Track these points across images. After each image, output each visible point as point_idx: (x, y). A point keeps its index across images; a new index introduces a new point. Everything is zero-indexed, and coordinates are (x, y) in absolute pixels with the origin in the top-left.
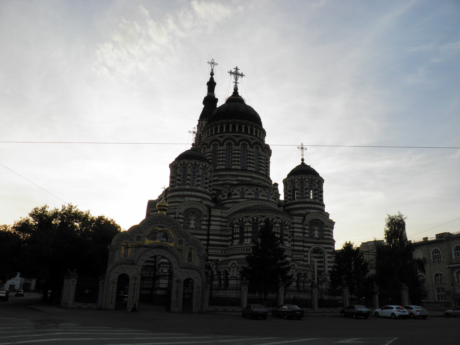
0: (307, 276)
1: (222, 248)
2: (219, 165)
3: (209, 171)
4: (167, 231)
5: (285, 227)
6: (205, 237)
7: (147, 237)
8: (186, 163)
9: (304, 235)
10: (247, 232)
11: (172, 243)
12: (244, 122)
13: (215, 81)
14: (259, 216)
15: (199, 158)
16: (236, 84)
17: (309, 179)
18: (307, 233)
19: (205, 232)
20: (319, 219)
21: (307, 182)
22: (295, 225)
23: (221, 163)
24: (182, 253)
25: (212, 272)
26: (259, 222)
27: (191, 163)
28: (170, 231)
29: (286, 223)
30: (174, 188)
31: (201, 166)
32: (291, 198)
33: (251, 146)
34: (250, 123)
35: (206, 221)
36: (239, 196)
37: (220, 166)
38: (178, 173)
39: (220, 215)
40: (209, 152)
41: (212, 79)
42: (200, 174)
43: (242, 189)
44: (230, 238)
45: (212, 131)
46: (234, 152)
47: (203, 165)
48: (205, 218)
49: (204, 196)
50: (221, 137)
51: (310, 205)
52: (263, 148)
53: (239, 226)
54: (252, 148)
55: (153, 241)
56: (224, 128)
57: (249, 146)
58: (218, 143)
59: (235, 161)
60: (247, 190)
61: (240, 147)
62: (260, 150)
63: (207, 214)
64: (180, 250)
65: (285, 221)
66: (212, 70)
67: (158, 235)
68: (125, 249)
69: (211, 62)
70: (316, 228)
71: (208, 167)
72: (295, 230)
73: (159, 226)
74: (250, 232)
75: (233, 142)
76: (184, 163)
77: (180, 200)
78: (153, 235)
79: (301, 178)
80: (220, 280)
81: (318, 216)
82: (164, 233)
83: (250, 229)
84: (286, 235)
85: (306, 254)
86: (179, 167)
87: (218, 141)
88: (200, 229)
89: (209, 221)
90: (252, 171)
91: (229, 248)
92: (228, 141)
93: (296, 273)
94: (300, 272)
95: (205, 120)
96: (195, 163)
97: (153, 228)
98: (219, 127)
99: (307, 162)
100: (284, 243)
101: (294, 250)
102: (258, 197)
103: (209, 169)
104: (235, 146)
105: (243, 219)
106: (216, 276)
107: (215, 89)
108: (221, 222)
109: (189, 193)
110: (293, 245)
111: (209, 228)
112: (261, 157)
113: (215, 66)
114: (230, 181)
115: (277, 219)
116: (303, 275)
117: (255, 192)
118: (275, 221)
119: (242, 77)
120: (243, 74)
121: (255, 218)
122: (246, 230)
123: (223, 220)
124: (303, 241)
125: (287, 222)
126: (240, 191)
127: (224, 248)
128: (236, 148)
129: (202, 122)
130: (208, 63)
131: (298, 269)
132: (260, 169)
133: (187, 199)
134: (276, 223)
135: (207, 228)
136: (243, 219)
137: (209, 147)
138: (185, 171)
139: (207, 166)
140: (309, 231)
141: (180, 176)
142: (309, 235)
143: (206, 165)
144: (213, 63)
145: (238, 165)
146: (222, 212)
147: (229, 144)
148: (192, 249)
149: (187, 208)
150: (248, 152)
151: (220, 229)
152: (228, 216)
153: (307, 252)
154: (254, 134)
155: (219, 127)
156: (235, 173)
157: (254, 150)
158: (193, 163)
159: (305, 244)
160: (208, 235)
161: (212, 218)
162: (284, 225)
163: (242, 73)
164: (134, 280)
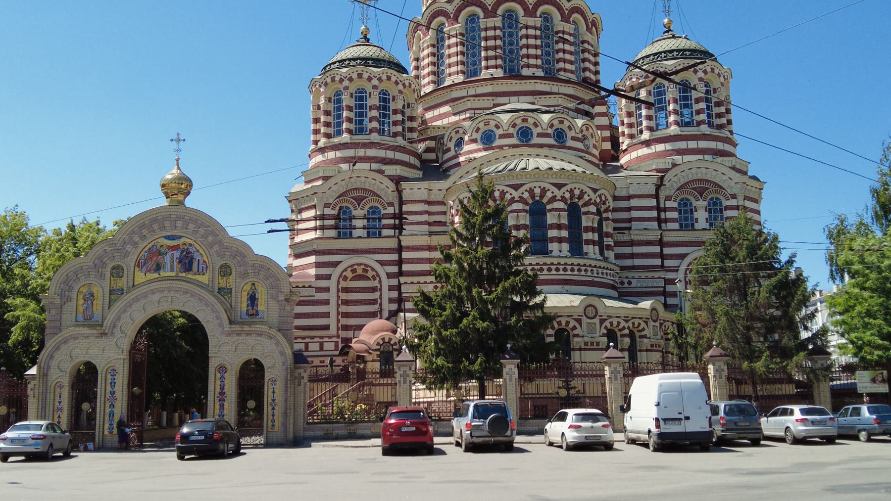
0: (643, 333)
3: (400, 92)
4: (191, 245)
5: (584, 210)
6: (395, 257)
7: (138, 266)
9: (663, 225)
11: (203, 274)
14: (507, 186)
15: (370, 62)
18: (673, 220)
19: (392, 243)
20: (708, 177)
22: (634, 203)
24: (231, 296)
26: (526, 205)
27: (349, 76)
28: (196, 245)
29: (586, 198)
31: (375, 82)
37: (453, 77)
39: (427, 199)
46: (483, 34)
48: (390, 210)
52: (567, 12)
54: (531, 16)
55: (156, 275)
57: (521, 12)
61: (497, 21)
63: (393, 197)
64: (225, 292)
65: (582, 193)
67: (168, 258)
68: (85, 300)
70: (698, 203)
71: (397, 83)
72: (635, 214)
73: (169, 236)
78: (154, 259)
81: (704, 171)
82: (182, 253)
84: (587, 229)
85: (670, 276)
88: (380, 236)
93: (603, 326)
94: (615, 324)
96: (360, 76)
97: (152, 243)
100: (585, 251)
101: (633, 268)
102: (530, 140)
103: (400, 87)
104: (485, 20)
108: (430, 213)
110: (632, 256)
114: (476, 111)
116: (626, 332)
117: (520, 129)
118: (549, 195)
124: (661, 243)
125: (589, 196)
126: (481, 132)
128: (489, 25)
131: (611, 317)
132: (559, 70)
134: (553, 199)
135: (397, 234)
139: (393, 79)
140: (680, 213)
142: (681, 225)
143: (389, 78)
145: (496, 67)
148: (256, 283)
149: (342, 190)
151: (428, 233)
153: (676, 270)
156: (488, 88)
157: (538, 21)
159: (667, 251)
160: (400, 249)
161: (405, 208)
162: (580, 203)
164: (111, 375)
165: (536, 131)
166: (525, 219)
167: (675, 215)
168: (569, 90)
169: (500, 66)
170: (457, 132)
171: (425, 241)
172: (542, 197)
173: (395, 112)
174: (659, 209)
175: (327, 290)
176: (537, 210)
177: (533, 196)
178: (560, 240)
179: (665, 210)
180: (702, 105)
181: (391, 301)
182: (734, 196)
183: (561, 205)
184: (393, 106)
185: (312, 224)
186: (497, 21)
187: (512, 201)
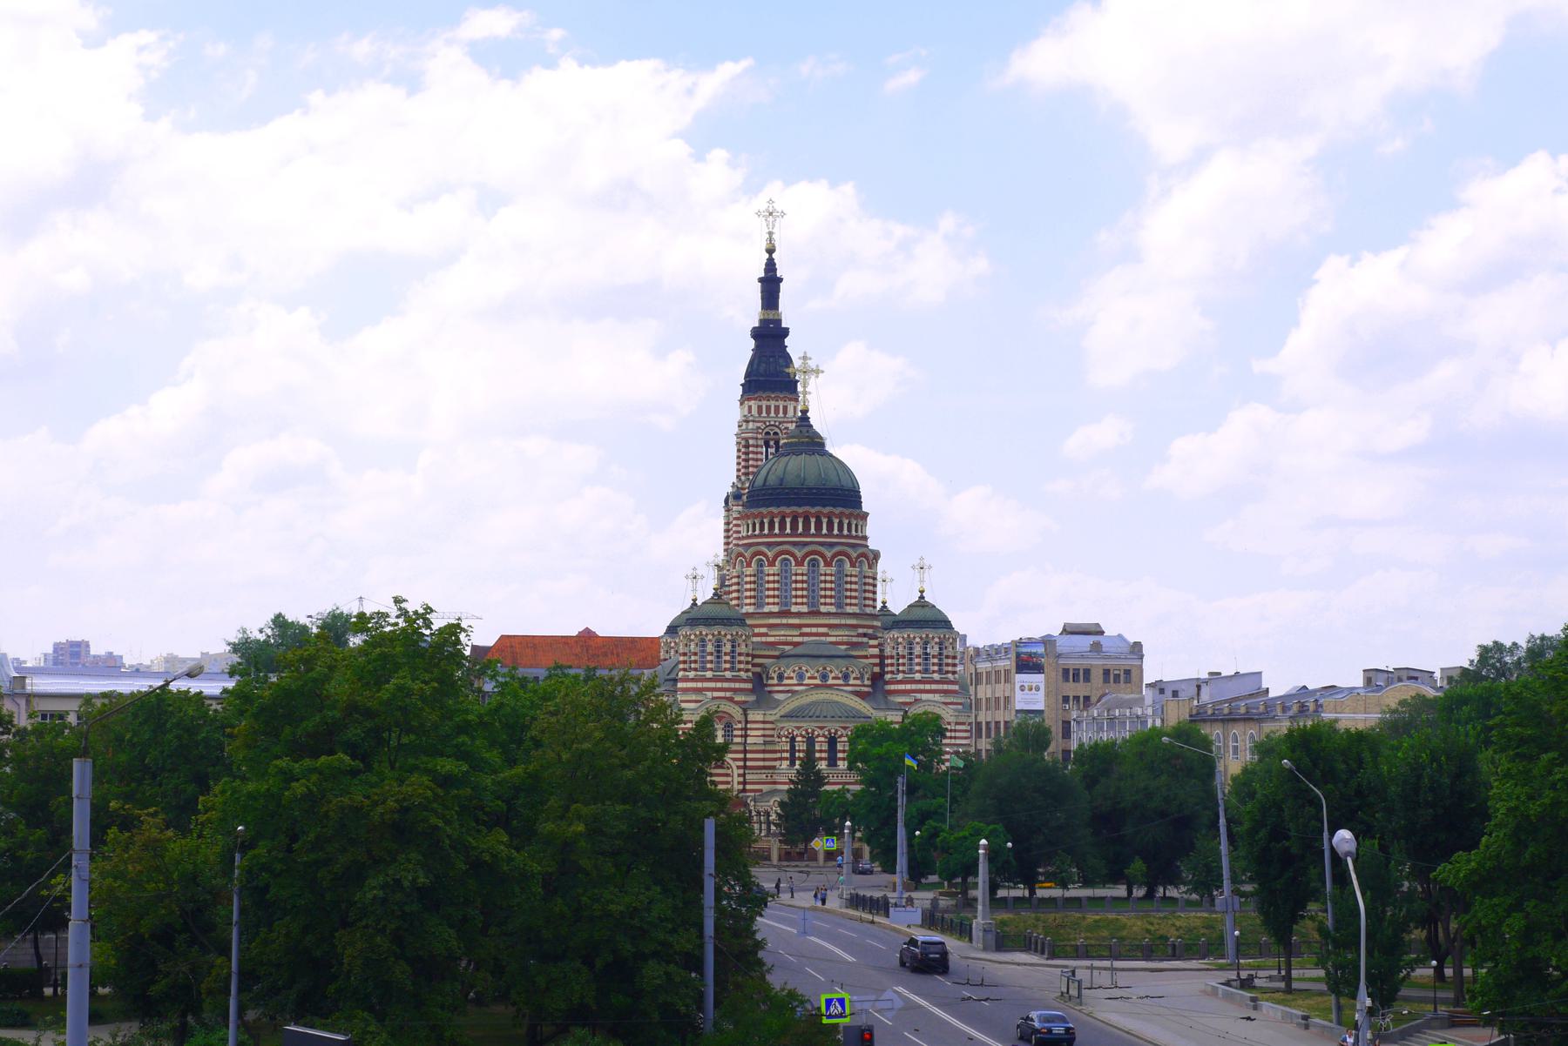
1: (766, 771)
2: (768, 604)
3: (744, 641)
6: (741, 756)
8: (704, 633)
10: (799, 751)
12: (813, 510)
16: (804, 397)
17: (921, 638)
19: (741, 748)
21: (918, 643)
23: (771, 600)
25: (750, 812)
30: (687, 673)
31: (729, 637)
32: (894, 669)
33: (828, 564)
34: (827, 510)
35: (742, 729)
36: (795, 682)
37: (770, 606)
38: (692, 651)
40: (750, 576)
41: (771, 266)
42: (728, 651)
43: (800, 668)
44: (778, 755)
45: (754, 530)
46: (794, 578)
47: (732, 635)
48: (739, 726)
49: (737, 685)
51: (921, 687)
53: (788, 740)
54: (829, 566)
56: (777, 525)
57: (822, 564)
58: (764, 559)
59: (796, 597)
60: (807, 671)
61: (804, 569)
62: (847, 565)
66: (770, 234)
69: (767, 210)
75: (791, 558)
76: (701, 633)
79: (909, 636)
80: (761, 823)
86: (693, 640)
87: (765, 555)
89: (746, 729)
90: (829, 614)
91: (776, 771)
92: (783, 556)
95: (755, 399)
96: (719, 633)
98: (766, 521)
103: (744, 637)
105: (793, 731)
106: (755, 818)
107: (781, 294)
108: (764, 729)
109: (712, 685)
111: (746, 741)
112: (849, 579)
113: (778, 219)
114: (788, 638)
115: (843, 731)
118: (839, 733)
119: (817, 377)
120: (821, 369)
121: (810, 730)
122: (797, 748)
127: (770, 771)
128: (798, 572)
130: (758, 214)
132: (847, 604)
133: (709, 694)
134: (841, 736)
136: (793, 731)
137: (749, 565)
138: (703, 646)
141: (695, 654)
143: (737, 633)
144: (771, 214)
145: (802, 604)
147: (785, 562)
150: (821, 575)
152: (776, 721)
154: (836, 532)
155: (766, 521)
157: (833, 569)
158: (716, 633)
160: (745, 752)
161: (749, 726)
163: (817, 366)
166: (825, 747)
168: (854, 622)
169: (806, 604)
170: (780, 669)
171: (762, 748)
173: (740, 654)
176: (832, 742)
177: (830, 734)
178: (844, 759)
180: (936, 661)
181: (739, 783)
182: (949, 723)
184: (738, 650)
186: (804, 569)
187: (818, 736)
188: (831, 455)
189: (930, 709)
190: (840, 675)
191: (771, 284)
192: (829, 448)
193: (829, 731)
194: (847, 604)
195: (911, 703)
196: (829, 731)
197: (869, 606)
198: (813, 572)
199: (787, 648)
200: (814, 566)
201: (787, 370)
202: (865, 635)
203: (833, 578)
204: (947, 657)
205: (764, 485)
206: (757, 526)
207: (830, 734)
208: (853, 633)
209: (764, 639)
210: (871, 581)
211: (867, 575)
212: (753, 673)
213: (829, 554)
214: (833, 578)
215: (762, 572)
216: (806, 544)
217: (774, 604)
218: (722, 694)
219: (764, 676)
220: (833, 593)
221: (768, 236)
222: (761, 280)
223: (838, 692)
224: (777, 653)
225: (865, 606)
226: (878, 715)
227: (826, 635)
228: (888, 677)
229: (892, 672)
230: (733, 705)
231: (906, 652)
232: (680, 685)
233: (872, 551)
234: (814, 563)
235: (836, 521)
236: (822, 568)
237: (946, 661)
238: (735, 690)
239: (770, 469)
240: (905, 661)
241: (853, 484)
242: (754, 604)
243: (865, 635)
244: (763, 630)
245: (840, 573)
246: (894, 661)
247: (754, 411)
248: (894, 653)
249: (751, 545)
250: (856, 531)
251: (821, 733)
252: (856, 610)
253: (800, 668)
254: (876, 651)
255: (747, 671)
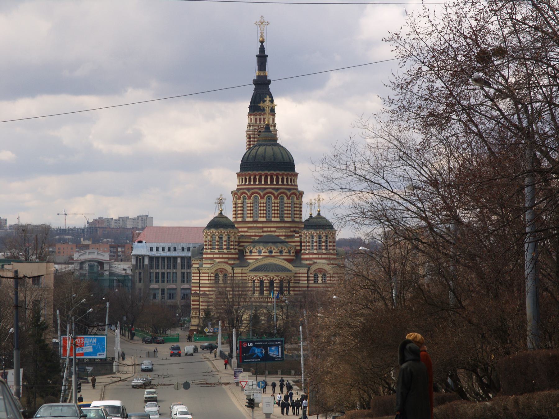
8: (214, 232)
13: (266, 54)
17: (317, 233)
20: (323, 268)
22: (300, 275)
23: (249, 215)
30: (207, 251)
31: (226, 233)
32: (305, 248)
33: (276, 198)
40: (240, 204)
41: (262, 49)
43: (259, 248)
45: (242, 182)
46: (259, 205)
48: (230, 275)
49: (230, 256)
50: (248, 189)
51: (317, 256)
57: (273, 198)
59: (261, 214)
60: (263, 249)
61: (264, 201)
62: (285, 198)
63: (231, 271)
66: (262, 33)
74: (258, 287)
75: (259, 196)
76: (213, 231)
77: (212, 262)
79: (311, 232)
83: (258, 285)
86: (209, 235)
87: (247, 194)
89: (233, 277)
95: (254, 115)
96: (221, 232)
99: (322, 214)
103: (233, 234)
112: (286, 205)
118: (275, 279)
123: (244, 275)
128: (262, 202)
129: (252, 117)
130: (256, 23)
132: (285, 217)
133: (217, 260)
134: (276, 280)
137: (239, 199)
143: (230, 232)
144: (262, 23)
145: (264, 217)
146: (242, 270)
154: (280, 183)
155: (247, 178)
156: (261, 225)
158: (220, 232)
161: (235, 275)
165: (274, 251)
166: (268, 285)
167: (313, 278)
169: (265, 217)
172: (273, 279)
174: (308, 277)
175: (212, 298)
177: (270, 279)
179: (310, 277)
182: (330, 274)
183: (278, 281)
185: (207, 278)
188: (280, 146)
189: (321, 267)
190: (278, 251)
191: (262, 58)
192: (279, 142)
193: (270, 277)
194: (285, 217)
195: (311, 264)
196: (270, 277)
197: (297, 217)
198: (269, 202)
199: (257, 238)
200: (269, 199)
201: (259, 105)
202: (294, 231)
203: (278, 205)
204: (330, 242)
205: (247, 160)
206: (244, 180)
207: (270, 279)
208: (289, 231)
209: (246, 234)
210: (298, 206)
211: (296, 203)
212: (239, 250)
213: (276, 194)
214: (278, 205)
215: (245, 202)
216: (265, 189)
217: (250, 217)
218: (223, 260)
219: (244, 251)
220: (278, 212)
221: (260, 34)
222: (257, 56)
223: (278, 260)
224: (251, 240)
225: (295, 217)
226: (294, 269)
227: (275, 232)
228: (303, 251)
229: (304, 249)
230: (227, 265)
231: (310, 240)
232: (204, 256)
233: (299, 192)
234: (269, 198)
235: (280, 178)
236: (273, 200)
237: (329, 244)
238: (229, 258)
239: (250, 153)
240: (310, 244)
241: (290, 159)
242: (242, 217)
243: (294, 231)
244: (246, 229)
245: (282, 202)
246: (305, 244)
247: (253, 121)
248: (305, 240)
249: (241, 189)
250: (291, 182)
251: (266, 278)
252: (290, 220)
253: (259, 248)
254: (298, 239)
255: (236, 249)
